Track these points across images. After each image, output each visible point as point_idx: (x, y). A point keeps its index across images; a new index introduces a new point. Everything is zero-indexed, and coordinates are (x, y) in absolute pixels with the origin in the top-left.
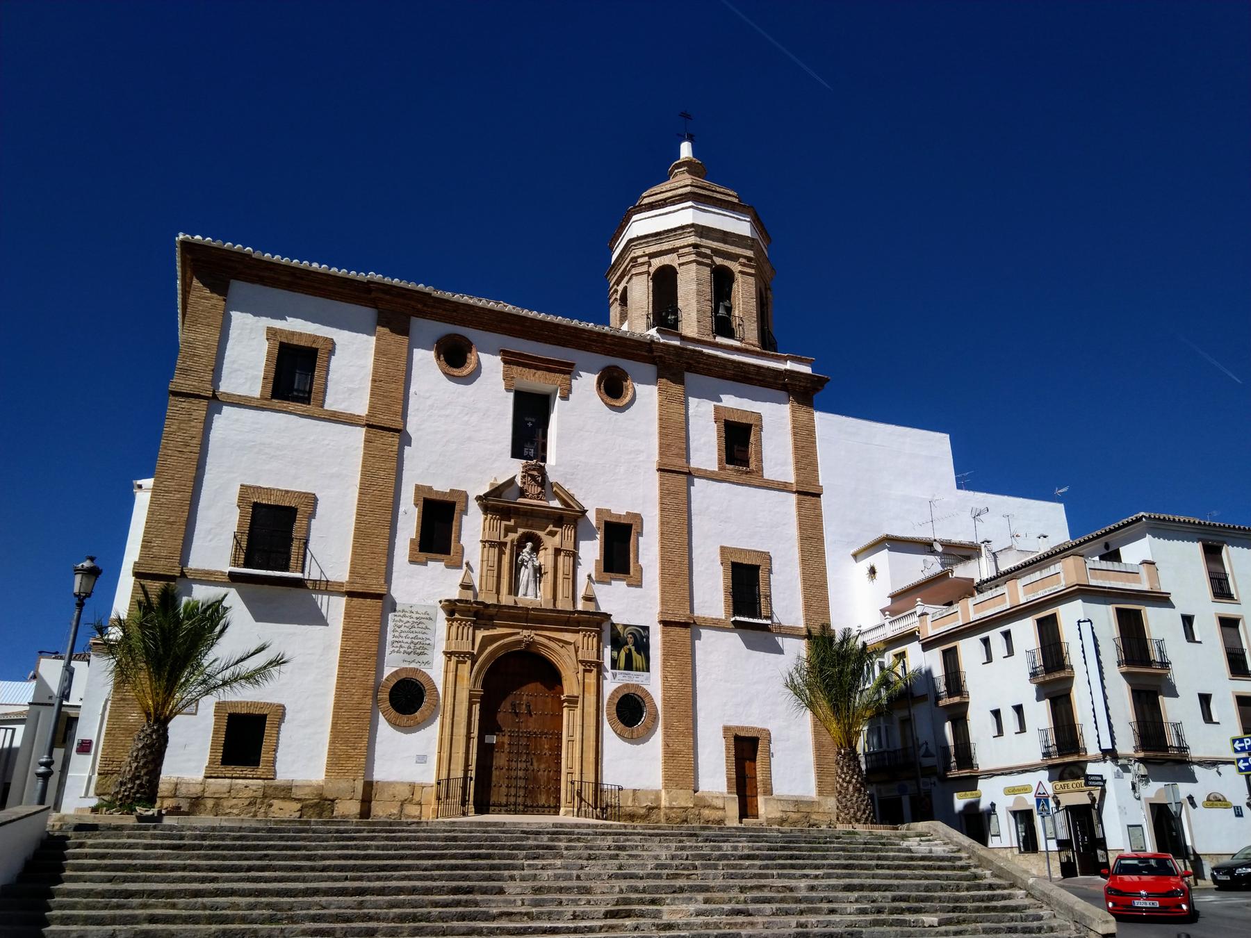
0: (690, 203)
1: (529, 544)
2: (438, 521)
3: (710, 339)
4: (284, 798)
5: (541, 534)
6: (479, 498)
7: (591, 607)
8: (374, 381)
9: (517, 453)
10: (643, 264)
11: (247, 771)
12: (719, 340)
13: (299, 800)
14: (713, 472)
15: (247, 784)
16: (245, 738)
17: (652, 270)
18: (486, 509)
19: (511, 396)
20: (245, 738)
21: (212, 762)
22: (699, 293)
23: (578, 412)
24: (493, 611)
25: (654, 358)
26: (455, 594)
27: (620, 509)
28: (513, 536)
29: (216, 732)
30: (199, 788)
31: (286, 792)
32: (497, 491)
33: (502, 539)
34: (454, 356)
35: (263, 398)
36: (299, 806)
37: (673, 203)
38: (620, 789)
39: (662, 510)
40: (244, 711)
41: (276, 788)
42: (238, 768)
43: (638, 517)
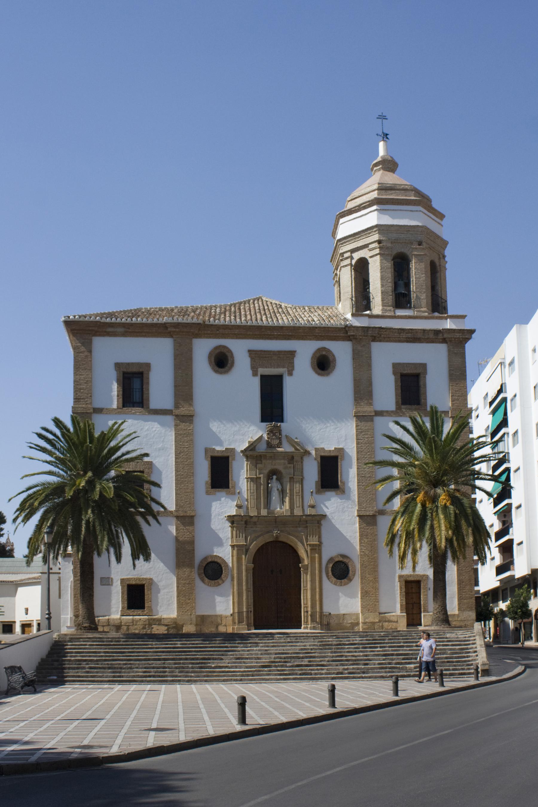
0: (375, 207)
1: (275, 477)
2: (220, 473)
3: (392, 314)
4: (159, 625)
5: (280, 468)
6: (242, 451)
7: (313, 512)
8: (175, 386)
9: (265, 418)
10: (347, 258)
11: (140, 611)
12: (400, 312)
13: (166, 625)
14: (392, 412)
15: (140, 617)
16: (136, 595)
17: (354, 262)
18: (247, 457)
19: (257, 381)
20: (136, 595)
21: (123, 608)
22: (382, 278)
23: (300, 385)
24: (255, 519)
25: (349, 336)
26: (233, 512)
27: (330, 446)
28: (266, 472)
29: (123, 593)
30: (119, 621)
31: (159, 621)
32: (252, 447)
33: (258, 476)
34: (221, 361)
35: (118, 408)
36: (166, 628)
37: (365, 208)
38: (330, 614)
39: (358, 444)
40: (134, 583)
41: (154, 619)
42: (136, 610)
43: (341, 450)
